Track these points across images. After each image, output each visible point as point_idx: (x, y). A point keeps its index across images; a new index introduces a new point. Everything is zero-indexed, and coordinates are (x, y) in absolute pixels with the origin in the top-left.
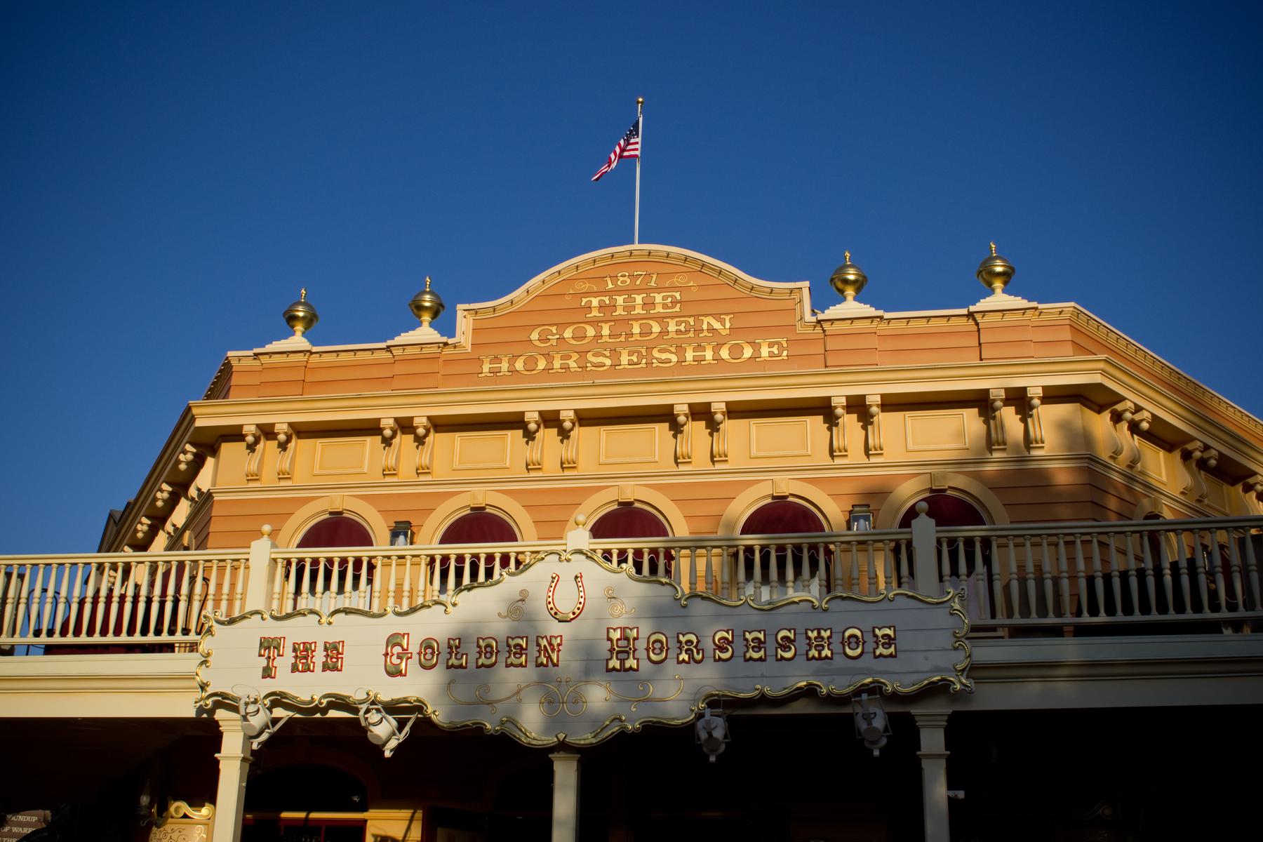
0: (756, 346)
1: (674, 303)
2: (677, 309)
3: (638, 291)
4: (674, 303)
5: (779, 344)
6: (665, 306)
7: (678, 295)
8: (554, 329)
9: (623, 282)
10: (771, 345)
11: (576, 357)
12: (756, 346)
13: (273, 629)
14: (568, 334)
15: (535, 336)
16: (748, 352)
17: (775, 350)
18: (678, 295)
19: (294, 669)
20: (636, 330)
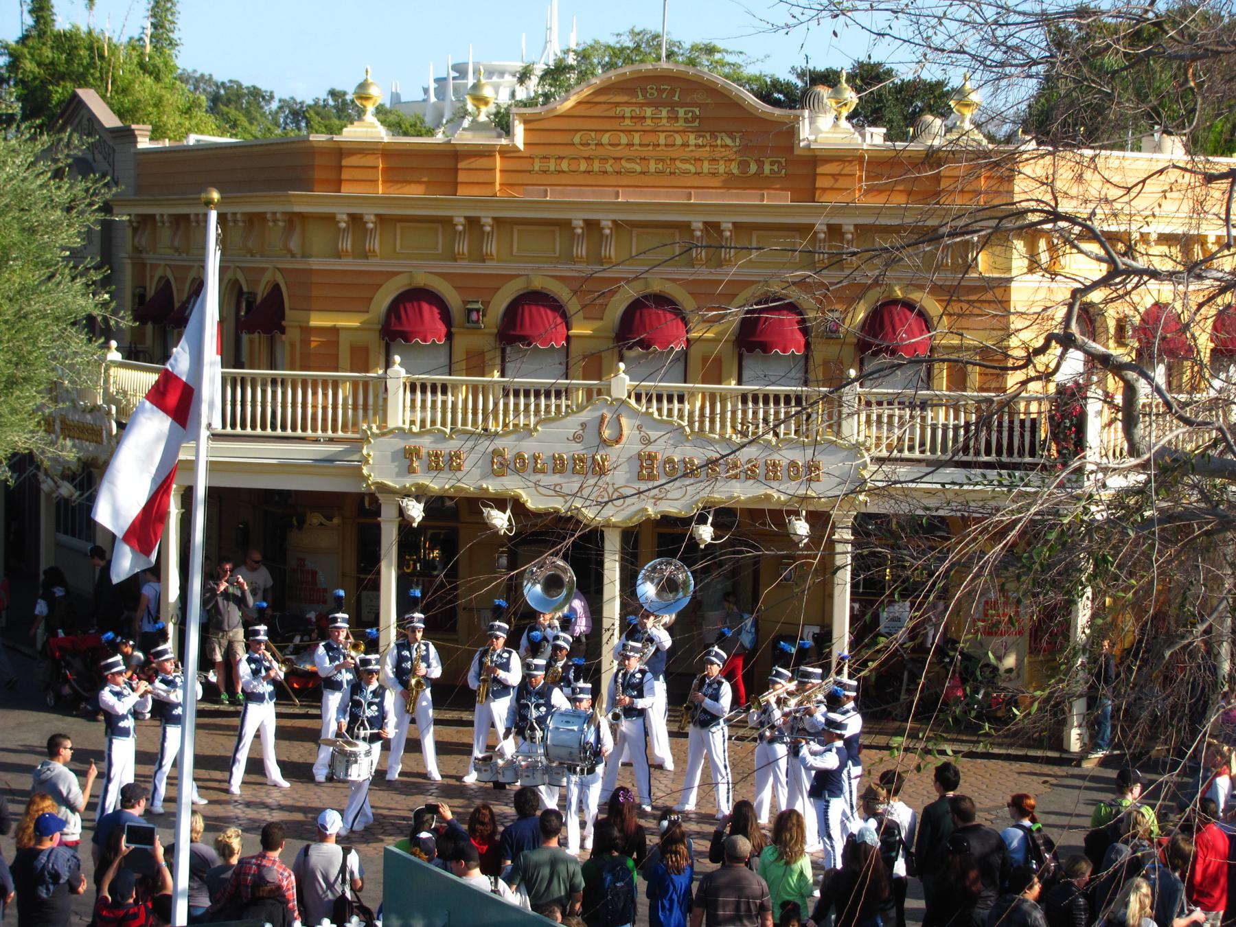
0: (760, 164)
1: (694, 118)
2: (696, 124)
3: (664, 105)
4: (694, 118)
5: (779, 163)
6: (686, 120)
7: (697, 110)
8: (593, 134)
9: (652, 94)
10: (772, 163)
11: (611, 161)
12: (760, 164)
13: (412, 443)
14: (605, 139)
15: (577, 140)
16: (753, 168)
17: (775, 168)
18: (697, 110)
19: (430, 469)
20: (662, 141)
